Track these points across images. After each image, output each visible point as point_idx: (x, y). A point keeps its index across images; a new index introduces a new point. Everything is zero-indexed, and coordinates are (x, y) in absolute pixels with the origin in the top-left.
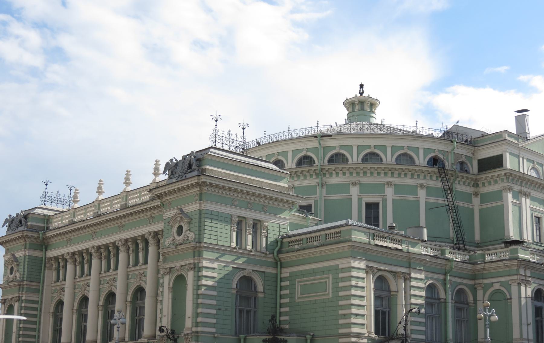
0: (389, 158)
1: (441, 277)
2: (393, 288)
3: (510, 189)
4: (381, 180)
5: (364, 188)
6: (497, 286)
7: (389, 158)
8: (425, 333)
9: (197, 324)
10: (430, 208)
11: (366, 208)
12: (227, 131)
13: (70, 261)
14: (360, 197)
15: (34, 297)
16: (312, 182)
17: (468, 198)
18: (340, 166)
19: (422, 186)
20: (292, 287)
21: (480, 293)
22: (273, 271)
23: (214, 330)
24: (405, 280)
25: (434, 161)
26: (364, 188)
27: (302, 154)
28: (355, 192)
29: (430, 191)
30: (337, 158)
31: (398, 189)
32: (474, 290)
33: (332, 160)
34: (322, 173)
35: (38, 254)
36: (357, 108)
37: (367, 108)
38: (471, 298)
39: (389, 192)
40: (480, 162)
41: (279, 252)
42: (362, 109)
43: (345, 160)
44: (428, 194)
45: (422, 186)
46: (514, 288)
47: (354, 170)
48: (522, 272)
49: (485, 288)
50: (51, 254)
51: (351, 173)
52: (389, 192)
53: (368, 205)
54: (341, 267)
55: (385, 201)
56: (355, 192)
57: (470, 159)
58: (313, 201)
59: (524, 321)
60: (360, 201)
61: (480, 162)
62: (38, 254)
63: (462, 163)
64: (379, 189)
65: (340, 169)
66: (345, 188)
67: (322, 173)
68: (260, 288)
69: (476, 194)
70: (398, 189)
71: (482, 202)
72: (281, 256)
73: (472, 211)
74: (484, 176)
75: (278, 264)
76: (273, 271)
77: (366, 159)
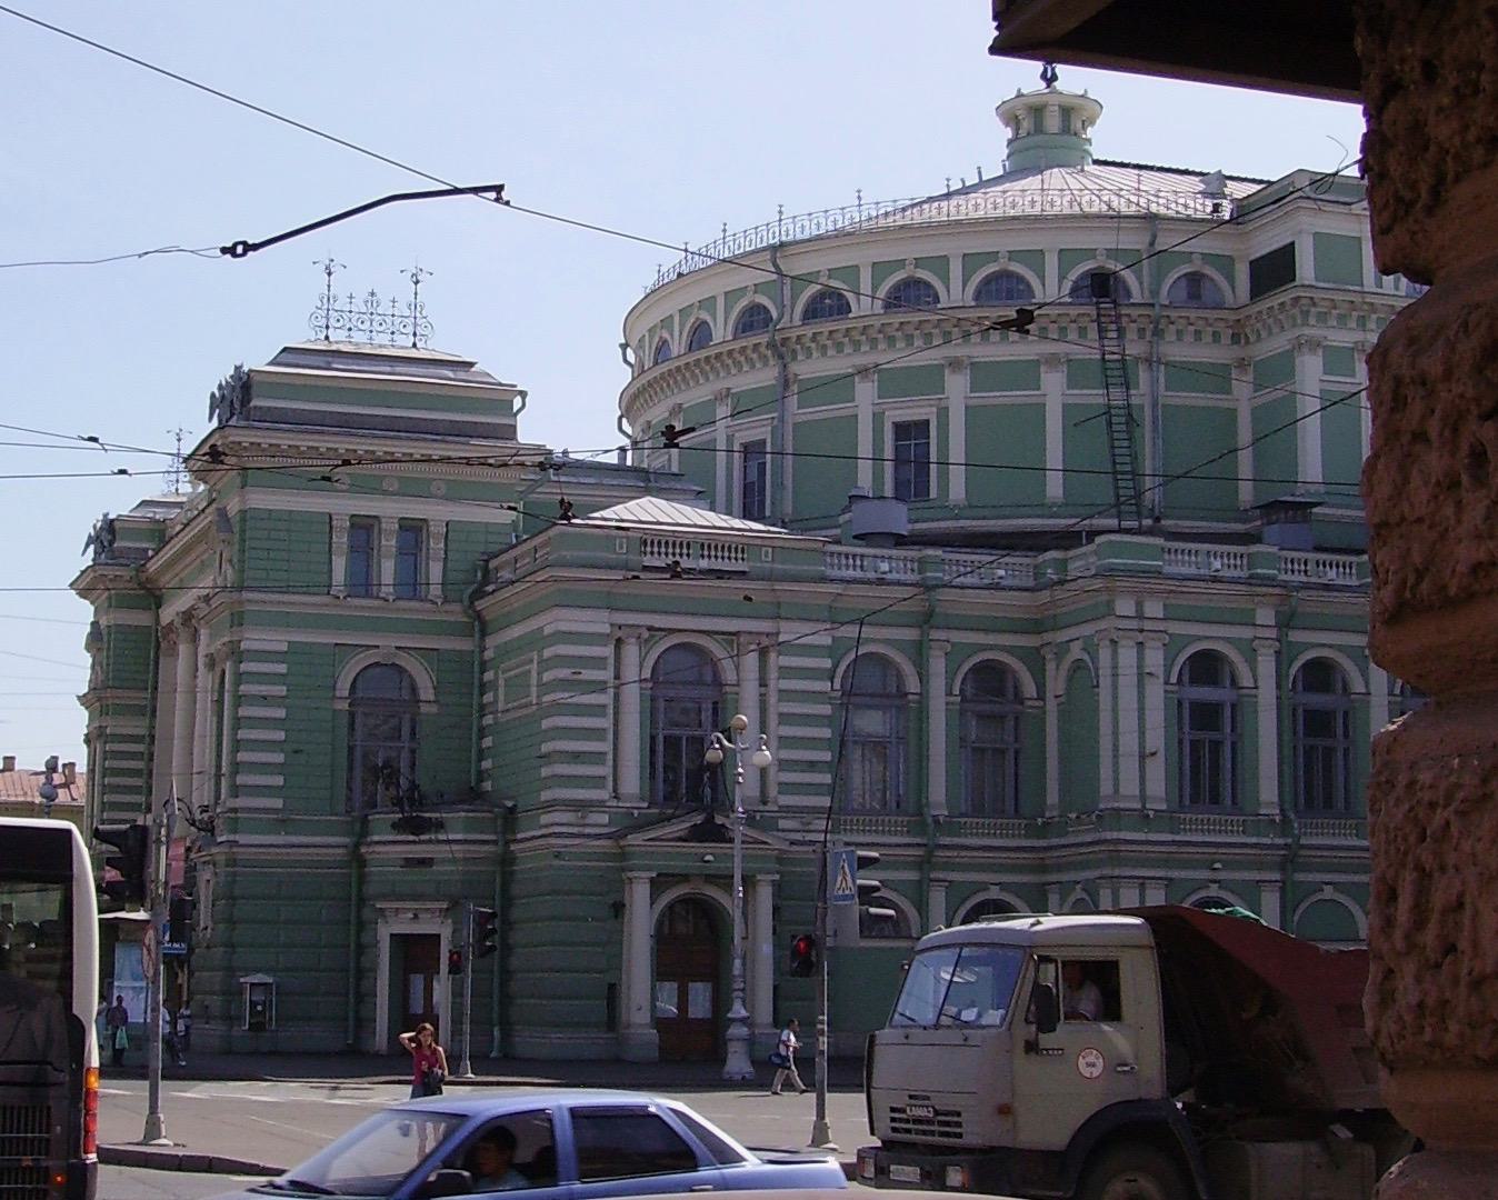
0: (956, 292)
1: (910, 634)
2: (729, 676)
3: (1315, 345)
4: (932, 357)
5: (894, 383)
6: (1076, 651)
7: (956, 292)
8: (831, 790)
9: (236, 791)
10: (1075, 420)
11: (897, 438)
12: (366, 296)
13: (184, 634)
14: (877, 409)
15: (137, 727)
16: (766, 376)
17: (1218, 377)
18: (916, 318)
19: (1052, 361)
20: (494, 685)
21: (1050, 666)
22: (464, 645)
23: (279, 803)
24: (763, 653)
25: (1100, 286)
26: (894, 383)
27: (992, 268)
28: (866, 392)
29: (1076, 374)
30: (829, 305)
31: (984, 375)
32: (1035, 660)
33: (811, 313)
34: (782, 351)
35: (141, 619)
36: (1026, 125)
37: (1053, 122)
38: (1029, 689)
39: (957, 388)
40: (1255, 265)
41: (479, 594)
42: (1039, 129)
43: (843, 308)
44: (1072, 382)
45: (1052, 361)
46: (1104, 655)
47: (868, 335)
48: (1125, 606)
49: (1059, 657)
50: (168, 614)
51: (857, 345)
52: (957, 388)
53: (902, 430)
54: (547, 631)
55: (943, 413)
56: (866, 392)
57: (1225, 263)
58: (934, 409)
59: (1129, 742)
60: (878, 418)
61: (1255, 265)
62: (141, 619)
63: (1195, 279)
64: (929, 381)
65: (897, 326)
66: (840, 386)
67: (782, 351)
68: (426, 693)
69: (1242, 364)
70: (984, 375)
71: (1258, 387)
72: (480, 605)
73: (1232, 414)
74: (1264, 305)
75: (481, 626)
76: (464, 645)
77: (895, 300)
